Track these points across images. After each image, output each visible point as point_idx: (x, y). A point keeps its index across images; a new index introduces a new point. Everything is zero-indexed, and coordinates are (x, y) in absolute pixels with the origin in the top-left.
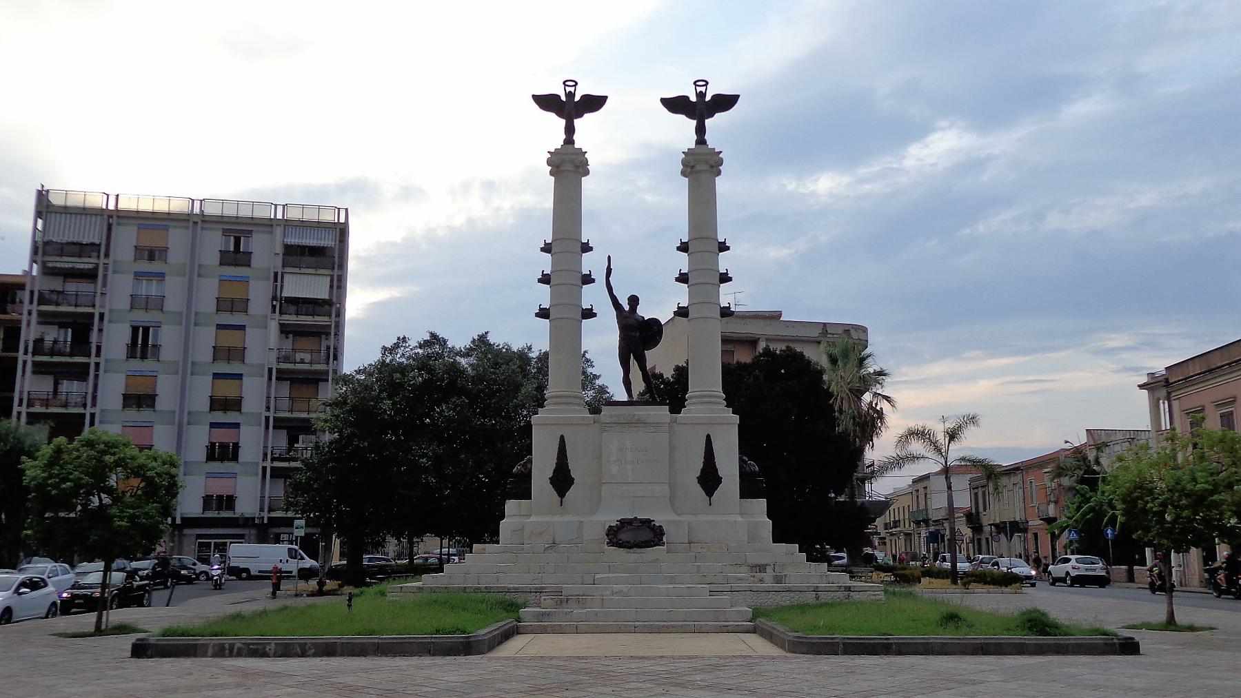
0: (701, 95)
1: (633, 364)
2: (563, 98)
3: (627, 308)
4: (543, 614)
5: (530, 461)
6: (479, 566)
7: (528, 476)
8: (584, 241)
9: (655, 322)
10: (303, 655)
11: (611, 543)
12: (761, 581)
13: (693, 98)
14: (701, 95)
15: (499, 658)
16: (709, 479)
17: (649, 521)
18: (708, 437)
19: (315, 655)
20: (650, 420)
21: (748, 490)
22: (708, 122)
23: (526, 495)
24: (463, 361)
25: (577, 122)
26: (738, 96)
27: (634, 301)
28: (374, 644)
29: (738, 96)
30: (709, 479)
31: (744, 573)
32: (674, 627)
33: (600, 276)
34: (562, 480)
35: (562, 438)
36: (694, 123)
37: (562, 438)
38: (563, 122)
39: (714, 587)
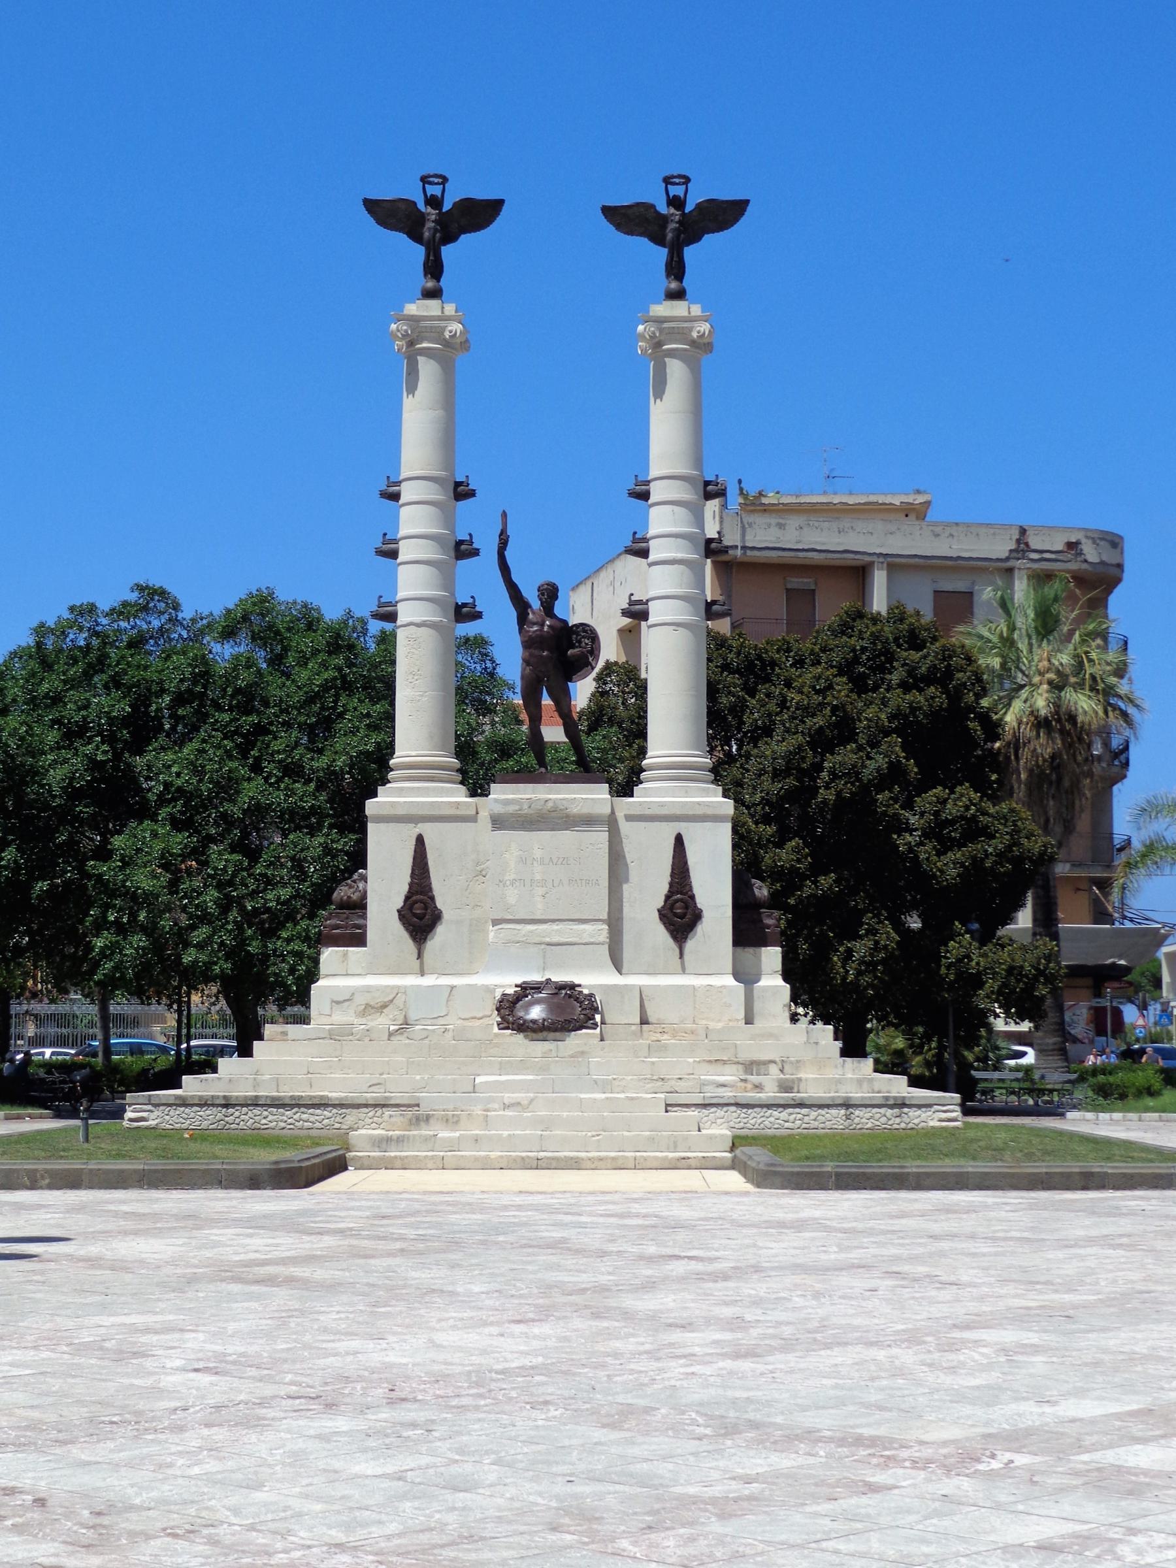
0: (676, 203)
1: (547, 701)
2: (421, 206)
3: (536, 604)
4: (389, 1140)
5: (364, 878)
6: (283, 1059)
7: (359, 906)
9: (588, 633)
10: (33, 1186)
11: (505, 1024)
12: (758, 1087)
13: (663, 208)
15: (323, 1193)
16: (680, 916)
17: (573, 987)
18: (679, 840)
19: (50, 1187)
21: (747, 931)
22: (690, 252)
23: (358, 939)
24: (223, 653)
25: (447, 251)
26: (747, 202)
27: (550, 594)
28: (135, 1171)
29: (747, 202)
30: (680, 916)
31: (730, 1075)
32: (601, 1159)
33: (488, 545)
34: (420, 916)
35: (420, 840)
36: (662, 253)
37: (420, 840)
38: (418, 252)
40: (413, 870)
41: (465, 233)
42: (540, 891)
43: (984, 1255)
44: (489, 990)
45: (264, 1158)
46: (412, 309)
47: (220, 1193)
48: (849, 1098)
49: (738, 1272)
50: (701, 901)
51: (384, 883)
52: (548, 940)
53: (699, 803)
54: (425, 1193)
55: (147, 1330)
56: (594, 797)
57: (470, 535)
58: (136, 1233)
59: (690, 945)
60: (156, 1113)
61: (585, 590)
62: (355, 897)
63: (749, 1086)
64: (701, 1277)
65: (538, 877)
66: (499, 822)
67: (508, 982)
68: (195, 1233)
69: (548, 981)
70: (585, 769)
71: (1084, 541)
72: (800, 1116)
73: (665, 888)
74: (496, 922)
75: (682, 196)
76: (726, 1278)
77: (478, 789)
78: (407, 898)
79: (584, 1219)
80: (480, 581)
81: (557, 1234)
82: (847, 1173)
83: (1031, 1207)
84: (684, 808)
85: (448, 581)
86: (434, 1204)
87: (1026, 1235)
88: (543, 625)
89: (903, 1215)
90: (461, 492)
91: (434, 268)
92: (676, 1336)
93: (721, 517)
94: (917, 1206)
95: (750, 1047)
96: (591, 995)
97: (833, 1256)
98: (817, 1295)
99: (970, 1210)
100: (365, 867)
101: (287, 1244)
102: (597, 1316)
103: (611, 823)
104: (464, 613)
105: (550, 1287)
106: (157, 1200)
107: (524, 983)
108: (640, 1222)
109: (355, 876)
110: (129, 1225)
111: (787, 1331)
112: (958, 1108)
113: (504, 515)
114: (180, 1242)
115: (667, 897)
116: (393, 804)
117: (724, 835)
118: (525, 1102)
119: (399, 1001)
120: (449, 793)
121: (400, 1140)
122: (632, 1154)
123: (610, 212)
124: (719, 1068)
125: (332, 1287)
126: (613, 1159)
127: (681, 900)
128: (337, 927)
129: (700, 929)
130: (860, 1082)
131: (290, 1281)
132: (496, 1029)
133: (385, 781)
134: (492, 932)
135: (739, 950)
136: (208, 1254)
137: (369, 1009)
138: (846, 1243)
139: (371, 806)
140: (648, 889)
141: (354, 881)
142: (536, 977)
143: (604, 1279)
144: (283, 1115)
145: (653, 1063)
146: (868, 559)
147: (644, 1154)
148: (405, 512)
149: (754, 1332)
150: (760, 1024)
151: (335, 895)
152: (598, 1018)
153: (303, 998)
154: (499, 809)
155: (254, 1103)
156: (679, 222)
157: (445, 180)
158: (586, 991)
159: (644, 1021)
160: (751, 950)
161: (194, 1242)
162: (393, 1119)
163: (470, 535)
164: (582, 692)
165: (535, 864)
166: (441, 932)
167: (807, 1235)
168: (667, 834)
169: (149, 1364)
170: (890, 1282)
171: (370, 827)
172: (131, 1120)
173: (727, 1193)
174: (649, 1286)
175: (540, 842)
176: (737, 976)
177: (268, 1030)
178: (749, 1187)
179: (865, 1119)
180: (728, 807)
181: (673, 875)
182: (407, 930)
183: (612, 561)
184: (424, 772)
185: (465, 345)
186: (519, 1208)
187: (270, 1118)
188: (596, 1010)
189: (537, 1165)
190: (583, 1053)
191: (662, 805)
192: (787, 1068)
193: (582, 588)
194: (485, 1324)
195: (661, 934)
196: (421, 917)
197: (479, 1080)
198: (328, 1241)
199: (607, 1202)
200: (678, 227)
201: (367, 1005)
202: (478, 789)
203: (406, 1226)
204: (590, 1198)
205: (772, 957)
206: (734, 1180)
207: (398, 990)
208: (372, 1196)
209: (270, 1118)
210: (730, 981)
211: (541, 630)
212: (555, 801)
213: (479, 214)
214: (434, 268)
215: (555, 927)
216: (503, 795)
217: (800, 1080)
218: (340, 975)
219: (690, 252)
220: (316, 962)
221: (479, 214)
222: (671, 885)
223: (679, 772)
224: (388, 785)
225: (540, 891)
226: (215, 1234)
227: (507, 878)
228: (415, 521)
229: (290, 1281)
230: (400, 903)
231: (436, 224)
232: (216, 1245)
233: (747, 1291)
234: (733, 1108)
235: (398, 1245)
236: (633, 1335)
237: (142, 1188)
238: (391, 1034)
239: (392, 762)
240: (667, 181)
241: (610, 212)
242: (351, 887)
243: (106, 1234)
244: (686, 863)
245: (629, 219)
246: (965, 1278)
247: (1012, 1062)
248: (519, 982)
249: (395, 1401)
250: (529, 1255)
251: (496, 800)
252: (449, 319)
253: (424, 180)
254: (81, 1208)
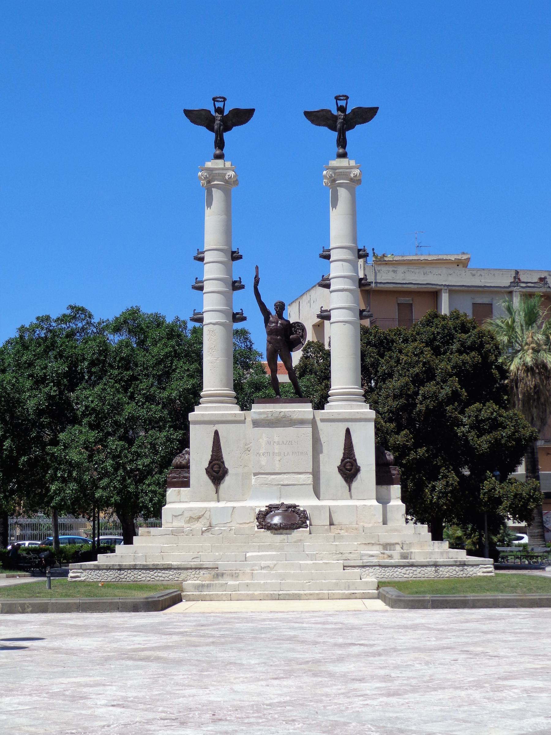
1: (280, 362)
2: (213, 113)
3: (273, 313)
4: (203, 586)
5: (188, 453)
6: (148, 545)
7: (186, 467)
8: (234, 249)
9: (300, 327)
10: (23, 612)
12: (390, 557)
13: (335, 112)
14: (342, 109)
15: (171, 614)
16: (349, 470)
17: (295, 506)
18: (348, 431)
19: (32, 612)
21: (383, 478)
22: (349, 134)
23: (186, 484)
26: (377, 108)
27: (281, 307)
28: (75, 603)
29: (377, 108)
31: (376, 551)
32: (311, 594)
33: (249, 283)
34: (217, 472)
35: (216, 433)
36: (335, 135)
37: (216, 433)
38: (212, 136)
39: (347, 563)
40: (213, 448)
41: (235, 126)
42: (278, 458)
43: (510, 641)
44: (252, 509)
45: (141, 596)
46: (209, 164)
47: (118, 614)
48: (436, 562)
49: (385, 652)
50: (359, 462)
51: (199, 455)
52: (282, 483)
53: (358, 413)
54: (223, 613)
55: (87, 685)
56: (304, 410)
57: (240, 278)
58: (77, 635)
59: (354, 484)
60: (84, 574)
61: (295, 306)
62: (184, 462)
63: (386, 556)
64: (367, 654)
65: (276, 451)
66: (256, 424)
67: (262, 505)
68: (107, 635)
69: (283, 504)
70: (299, 396)
71: (548, 277)
72: (412, 571)
73: (341, 456)
74: (255, 474)
75: (345, 106)
76: (380, 655)
77: (245, 406)
78: (210, 463)
79: (305, 625)
80: (245, 301)
81: (292, 633)
82: (437, 600)
83: (532, 616)
84: (350, 415)
85: (229, 302)
86: (227, 618)
87: (531, 630)
88: (277, 323)
89: (467, 621)
90: (235, 256)
91: (220, 144)
92: (357, 685)
93: (364, 268)
94: (474, 616)
95: (386, 537)
96: (304, 511)
97: (433, 643)
98: (427, 663)
99: (501, 618)
100: (189, 447)
101: (155, 640)
102: (315, 675)
103: (313, 423)
104: (237, 317)
105: (290, 660)
106: (87, 618)
107: (270, 505)
108: (333, 626)
109: (184, 452)
110: (74, 631)
111: (414, 682)
112: (492, 566)
113: (257, 268)
114: (100, 639)
115: (342, 461)
116: (202, 415)
117: (371, 428)
118: (272, 566)
119: (208, 514)
120: (231, 409)
121: (208, 586)
122: (327, 592)
123: (308, 114)
124: (370, 547)
125: (179, 662)
126: (318, 594)
127: (350, 462)
128: (175, 478)
129: (359, 476)
130: (442, 553)
131: (157, 659)
132: (256, 529)
134: (253, 479)
135: (379, 487)
136: (114, 645)
137: (191, 519)
138: (440, 636)
139: (191, 416)
140: (333, 456)
141: (183, 454)
142: (276, 502)
143: (318, 656)
144: (149, 574)
145: (336, 545)
146: (438, 287)
147: (333, 592)
148: (206, 267)
149: (397, 683)
150: (390, 524)
151: (173, 461)
152: (308, 522)
153: (158, 514)
154: (256, 417)
155: (134, 568)
156: (344, 119)
157: (225, 99)
158: (302, 509)
159: (331, 524)
160: (385, 487)
161: (107, 639)
162: (206, 575)
163: (240, 278)
164: (297, 356)
165: (275, 444)
166: (227, 479)
167: (419, 632)
168: (341, 429)
169: (89, 703)
170: (464, 656)
171: (191, 427)
172: (71, 577)
173: (376, 611)
174: (341, 659)
175: (277, 433)
176: (378, 500)
177: (141, 530)
178: (387, 608)
179: (445, 572)
180: (372, 414)
181: (345, 449)
182: (210, 478)
183: (309, 290)
184: (218, 398)
185: (236, 182)
186: (271, 620)
187: (143, 575)
188: (307, 518)
189: (279, 598)
190: (301, 540)
191: (339, 414)
192: (405, 547)
193: (294, 304)
194: (259, 680)
195: (339, 479)
196: (217, 472)
197: (248, 555)
198: (175, 638)
199: (316, 617)
200: (342, 121)
201: (191, 517)
202: (245, 406)
203: (214, 630)
204: (307, 615)
205: (396, 490)
206: (379, 604)
207: (206, 509)
208: (196, 615)
209: (143, 575)
210: (375, 503)
211: (277, 326)
212: (285, 412)
213: (242, 116)
214: (220, 144)
215: (285, 476)
216: (259, 410)
217: (411, 552)
218: (177, 502)
219: (349, 134)
220: (164, 496)
221: (242, 116)
222: (344, 454)
223: (347, 396)
224: (200, 405)
225: (278, 458)
226: (117, 635)
227: (261, 451)
228: (212, 271)
229: (157, 659)
230: (206, 465)
231: (221, 122)
232: (118, 641)
233: (391, 662)
234: (378, 568)
235: (211, 640)
236: (335, 685)
237: (78, 612)
238: (203, 532)
239: (202, 394)
240: (337, 98)
241: (308, 114)
242: (181, 457)
243: (62, 636)
244: (352, 443)
245: (318, 118)
246: (502, 654)
247: (516, 542)
248: (268, 505)
249: (216, 720)
250: (278, 644)
251: (255, 412)
252: (228, 169)
253: (214, 99)
254: (47, 623)
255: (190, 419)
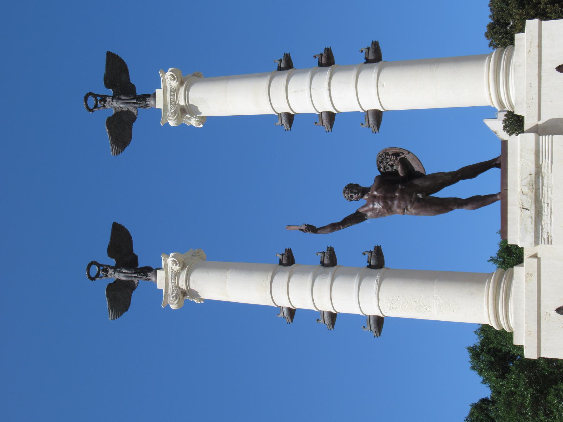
1: (445, 193)
20: (532, 168)
26: (109, 54)
27: (355, 190)
29: (109, 54)
90: (288, 260)
103: (538, 130)
116: (528, 333)
133: (509, 336)
139: (530, 354)
154: (530, 237)
180: (532, 24)
239: (496, 328)
255: (534, 356)
